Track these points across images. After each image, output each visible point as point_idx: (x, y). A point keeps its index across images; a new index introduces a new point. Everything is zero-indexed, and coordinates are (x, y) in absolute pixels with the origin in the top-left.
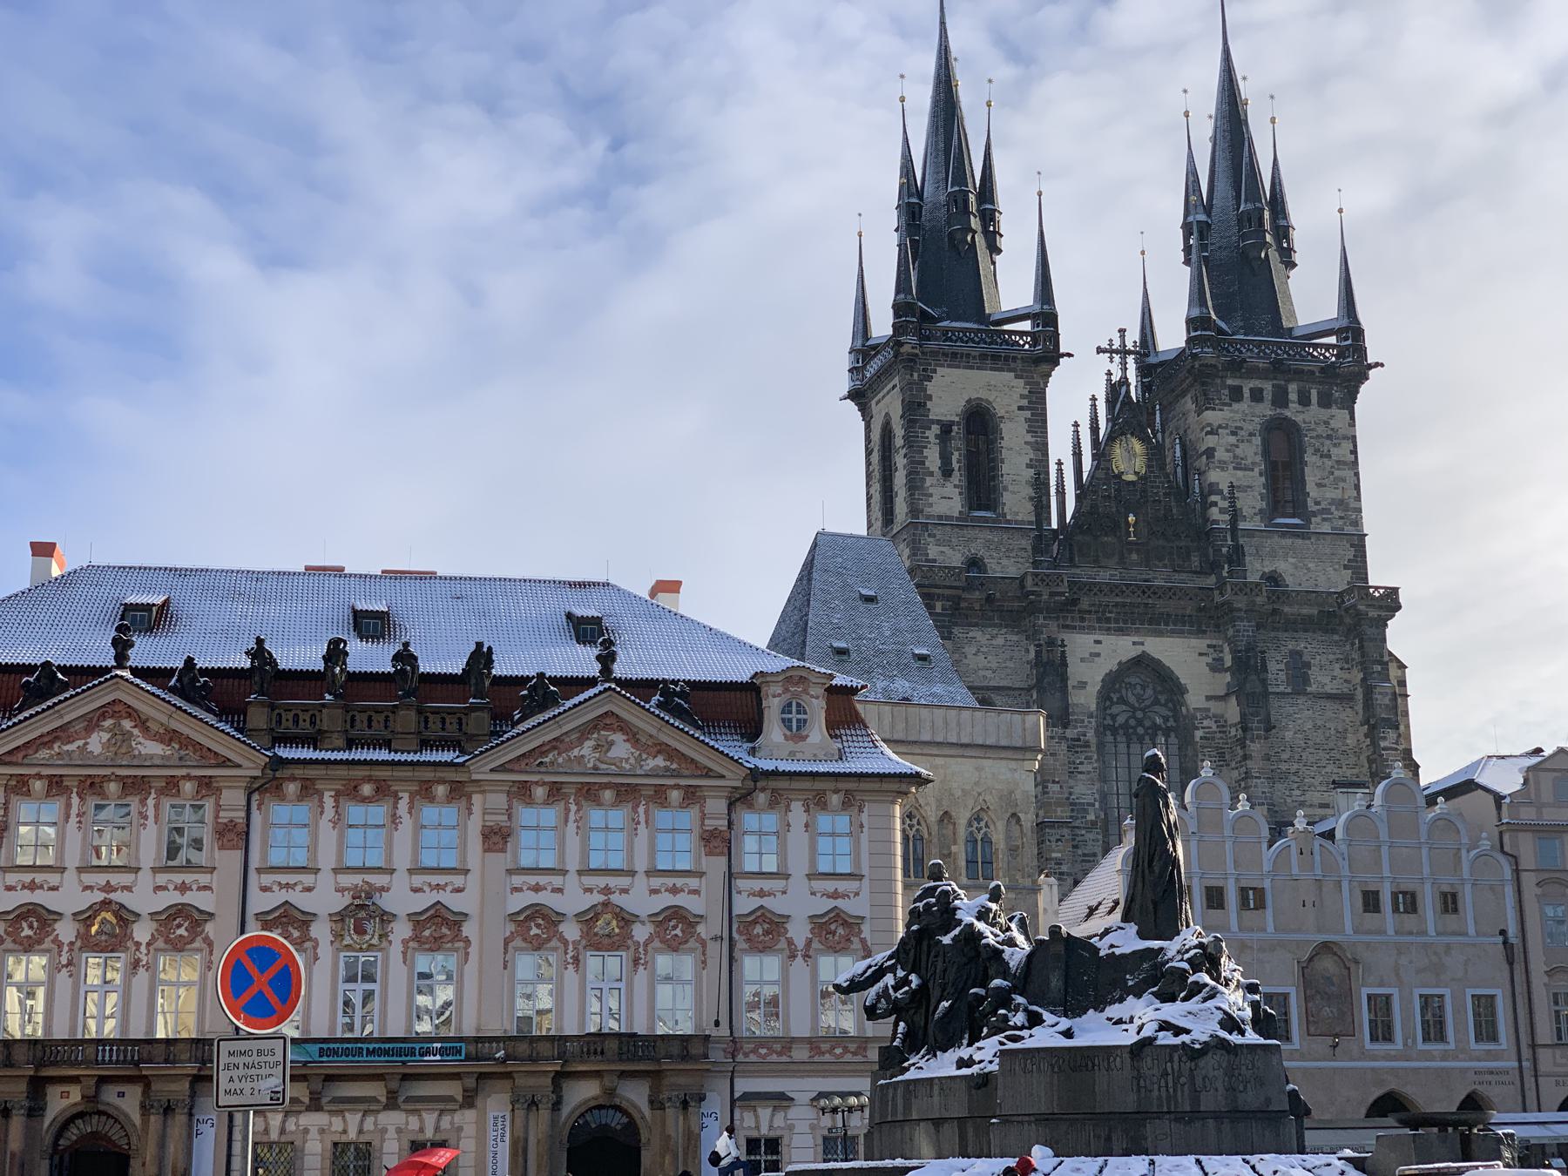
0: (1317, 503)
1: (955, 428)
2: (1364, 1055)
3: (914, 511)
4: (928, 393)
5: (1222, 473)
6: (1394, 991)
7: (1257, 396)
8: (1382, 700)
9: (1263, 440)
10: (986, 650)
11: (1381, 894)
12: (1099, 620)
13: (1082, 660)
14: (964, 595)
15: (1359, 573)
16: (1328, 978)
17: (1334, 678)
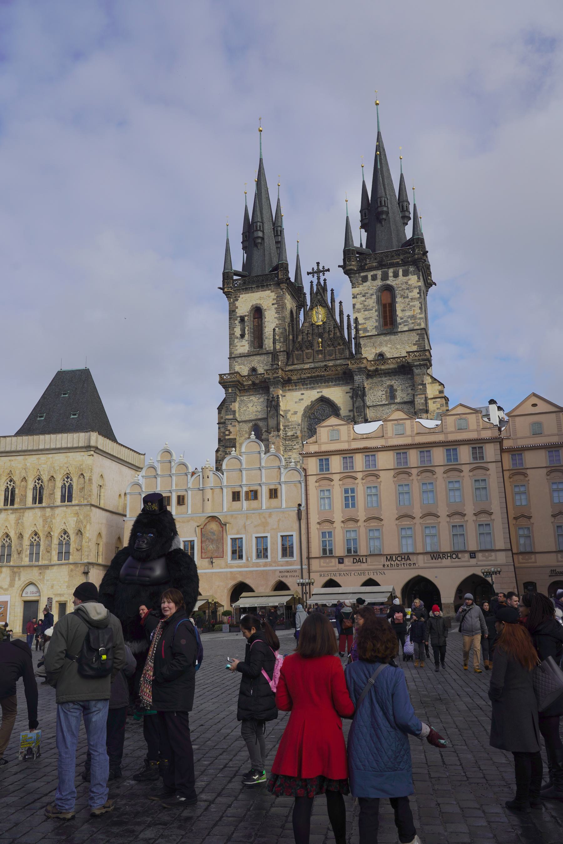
0: (402, 319)
1: (246, 318)
2: (227, 566)
3: (231, 353)
5: (357, 315)
6: (243, 536)
7: (374, 278)
8: (419, 400)
9: (378, 297)
10: (256, 404)
11: (241, 493)
12: (303, 385)
13: (296, 402)
14: (245, 383)
15: (421, 346)
16: (212, 532)
17: (408, 394)
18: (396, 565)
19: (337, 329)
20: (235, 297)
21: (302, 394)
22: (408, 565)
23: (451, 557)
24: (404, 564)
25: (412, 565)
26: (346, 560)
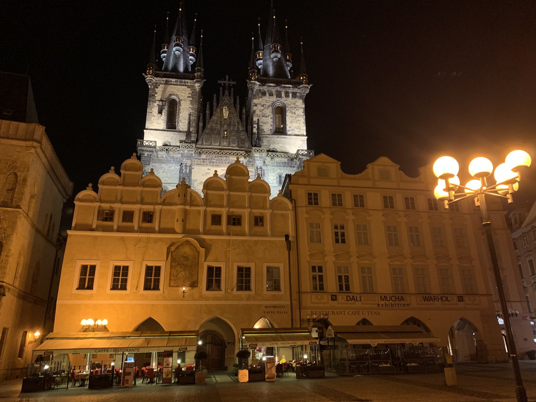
2: (201, 298)
4: (156, 92)
7: (271, 95)
9: (273, 109)
10: (166, 171)
12: (210, 162)
13: (203, 175)
16: (185, 257)
18: (390, 305)
19: (240, 125)
20: (155, 85)
21: (209, 169)
22: (402, 306)
23: (442, 299)
24: (398, 304)
25: (406, 305)
26: (340, 297)
